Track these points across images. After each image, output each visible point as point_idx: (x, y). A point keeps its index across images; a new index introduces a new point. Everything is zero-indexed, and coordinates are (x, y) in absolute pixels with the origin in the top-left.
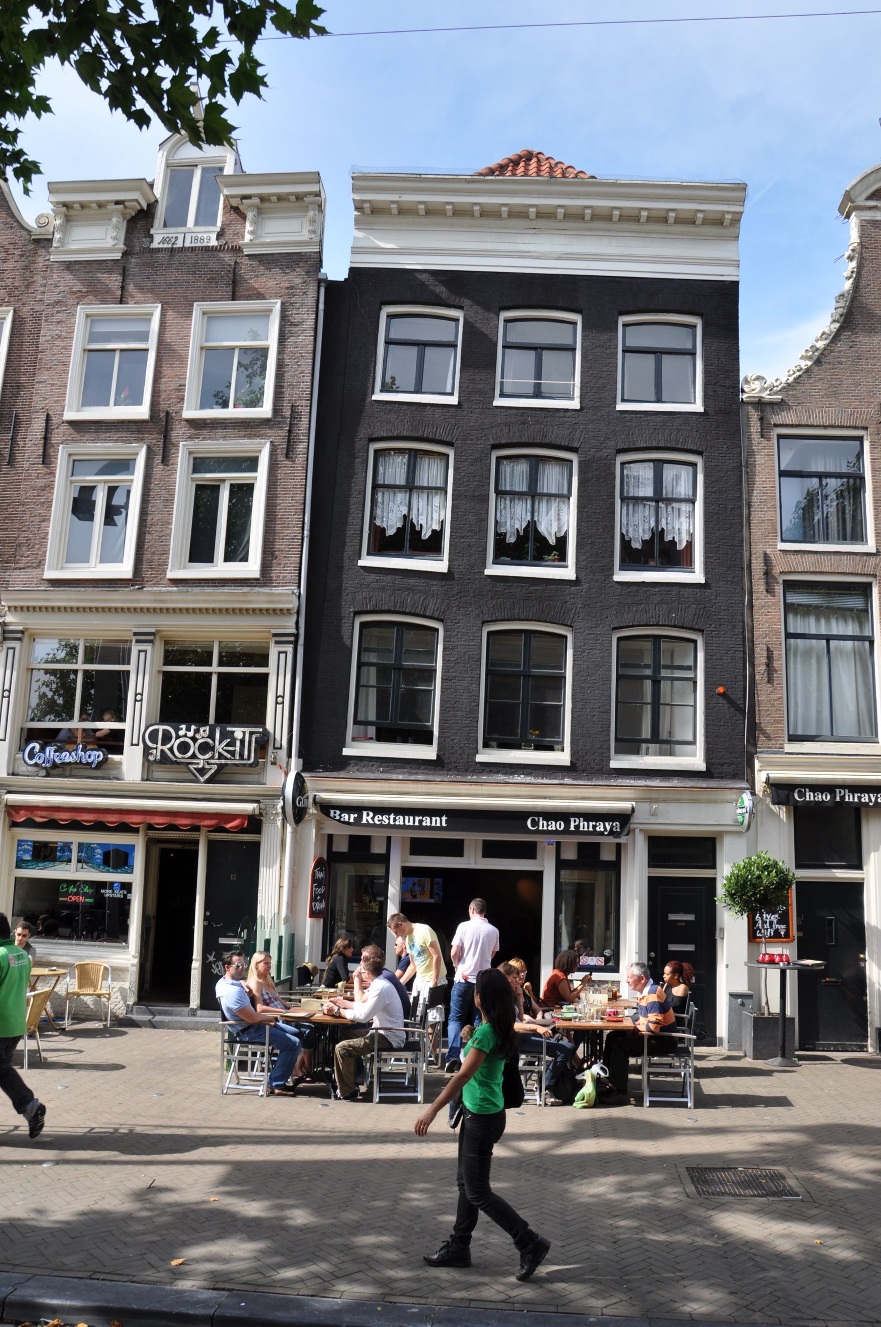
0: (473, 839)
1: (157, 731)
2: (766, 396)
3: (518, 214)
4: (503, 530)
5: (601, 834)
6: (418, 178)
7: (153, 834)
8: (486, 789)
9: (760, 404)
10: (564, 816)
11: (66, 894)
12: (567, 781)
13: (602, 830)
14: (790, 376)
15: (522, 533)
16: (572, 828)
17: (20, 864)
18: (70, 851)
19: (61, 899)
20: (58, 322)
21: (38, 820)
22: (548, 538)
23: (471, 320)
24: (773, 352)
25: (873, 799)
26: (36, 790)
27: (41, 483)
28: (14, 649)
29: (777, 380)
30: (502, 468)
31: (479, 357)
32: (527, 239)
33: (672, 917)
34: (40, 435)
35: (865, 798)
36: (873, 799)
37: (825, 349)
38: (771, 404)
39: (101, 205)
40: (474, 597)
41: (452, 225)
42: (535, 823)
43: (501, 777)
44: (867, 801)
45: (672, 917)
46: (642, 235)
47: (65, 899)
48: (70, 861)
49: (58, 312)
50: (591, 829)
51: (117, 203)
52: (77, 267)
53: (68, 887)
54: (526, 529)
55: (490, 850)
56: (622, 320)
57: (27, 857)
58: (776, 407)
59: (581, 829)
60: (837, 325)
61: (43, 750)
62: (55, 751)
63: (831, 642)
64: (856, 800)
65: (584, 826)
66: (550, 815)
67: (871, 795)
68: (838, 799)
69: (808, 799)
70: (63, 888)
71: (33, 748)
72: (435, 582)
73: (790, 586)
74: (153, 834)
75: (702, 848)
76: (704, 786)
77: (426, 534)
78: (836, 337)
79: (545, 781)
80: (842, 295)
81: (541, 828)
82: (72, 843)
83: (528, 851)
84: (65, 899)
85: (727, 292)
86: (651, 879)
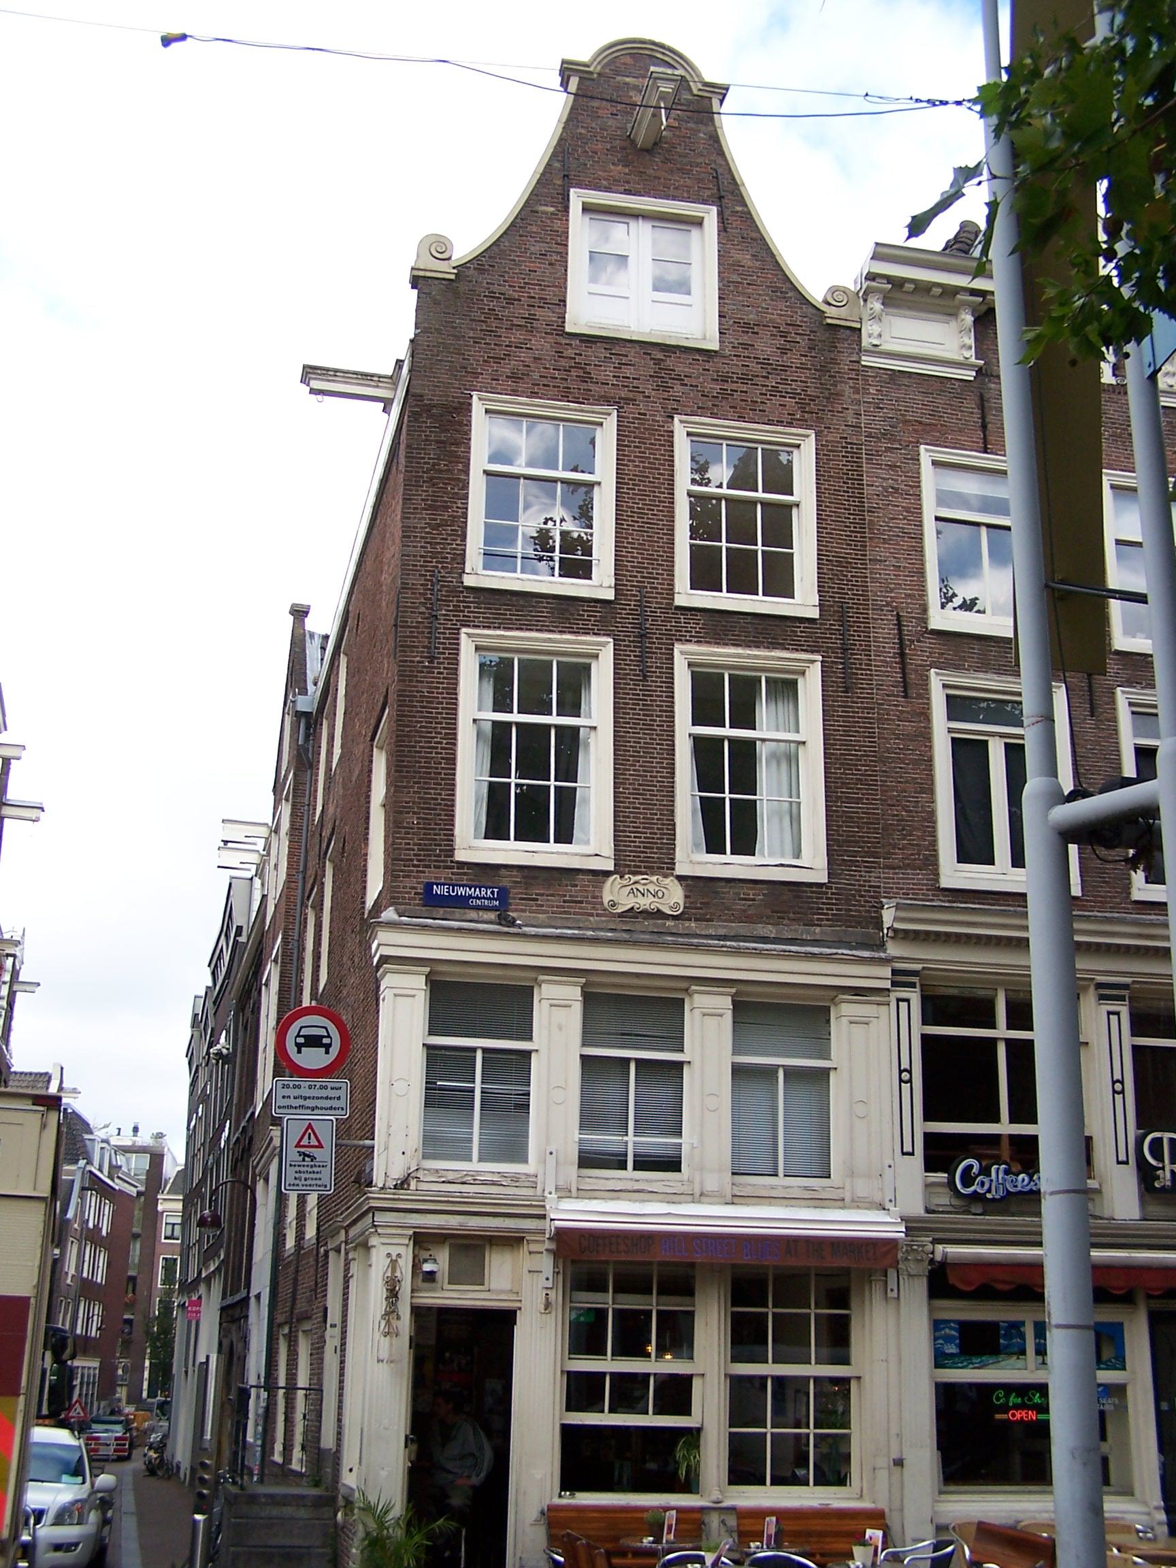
1: (1161, 1139)
7: (1157, 1305)
11: (1005, 1409)
17: (941, 1359)
18: (1022, 1336)
19: (998, 1416)
20: (892, 467)
21: (1000, 1287)
26: (978, 1236)
27: (908, 727)
28: (908, 1001)
34: (891, 649)
39: (950, 292)
47: (1004, 1416)
48: (1023, 1352)
49: (888, 449)
51: (974, 292)
52: (906, 381)
53: (1007, 1396)
57: (952, 1349)
61: (985, 1171)
62: (1007, 1172)
70: (998, 1399)
71: (970, 1167)
74: (1157, 1305)
82: (1023, 1323)
84: (1004, 1416)
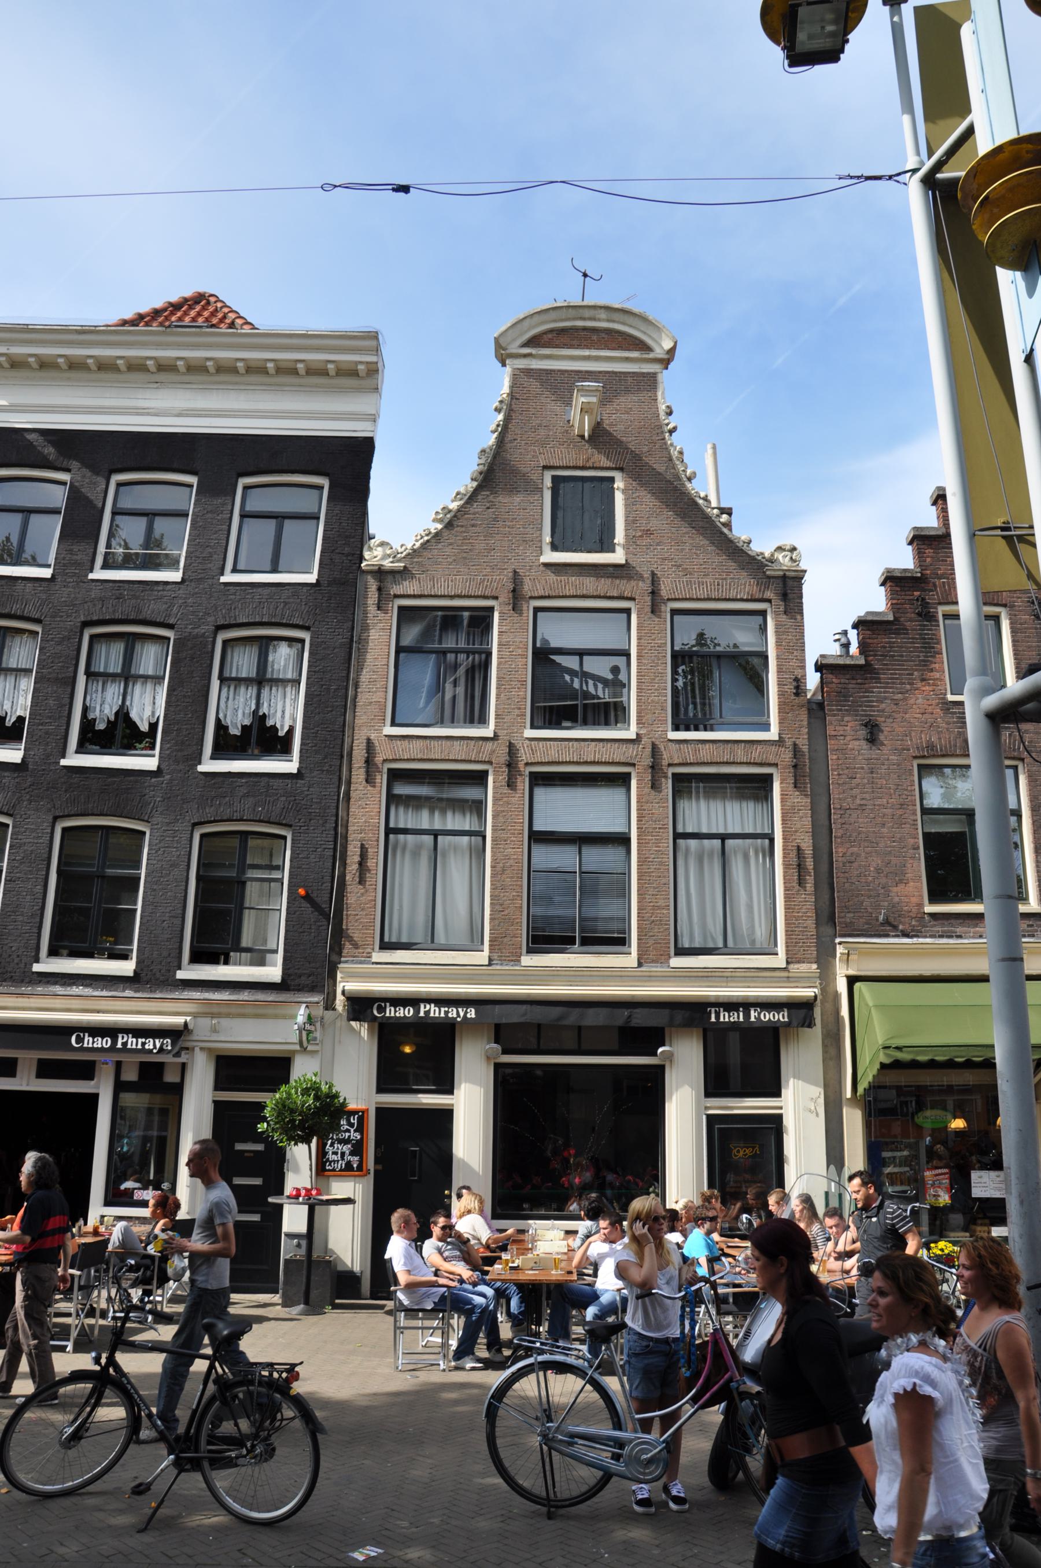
0: (28, 1058)
2: (387, 564)
3: (136, 367)
4: (91, 716)
5: (150, 1051)
6: (25, 329)
8: (34, 1002)
9: (380, 573)
10: (111, 1031)
12: (128, 993)
13: (151, 1047)
14: (417, 541)
15: (112, 718)
16: (119, 1046)
22: (139, 723)
23: (77, 484)
24: (401, 514)
25: (462, 1014)
29: (402, 546)
30: (97, 647)
31: (81, 523)
32: (148, 394)
33: (239, 1147)
35: (453, 1013)
36: (462, 1014)
37: (459, 511)
38: (393, 572)
40: (47, 790)
41: (69, 379)
42: (80, 1040)
43: (58, 989)
44: (455, 1016)
45: (239, 1147)
46: (273, 388)
50: (139, 1047)
54: (117, 714)
55: (46, 1070)
56: (243, 482)
58: (398, 576)
59: (129, 1046)
60: (475, 484)
63: (440, 838)
64: (442, 1015)
65: (132, 1043)
66: (97, 1031)
67: (460, 1010)
68: (422, 1014)
69: (388, 1015)
72: (6, 774)
73: (395, 776)
75: (272, 1069)
76: (270, 999)
77: (9, 722)
78: (472, 497)
79: (105, 993)
80: (483, 451)
81: (85, 1045)
83: (85, 1070)
85: (360, 451)
86: (217, 1104)
